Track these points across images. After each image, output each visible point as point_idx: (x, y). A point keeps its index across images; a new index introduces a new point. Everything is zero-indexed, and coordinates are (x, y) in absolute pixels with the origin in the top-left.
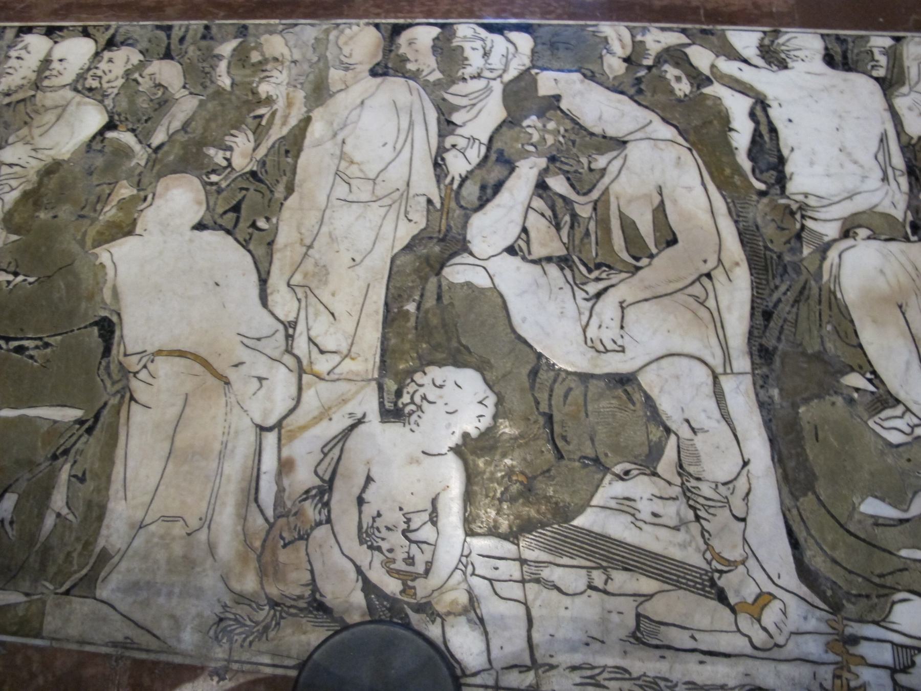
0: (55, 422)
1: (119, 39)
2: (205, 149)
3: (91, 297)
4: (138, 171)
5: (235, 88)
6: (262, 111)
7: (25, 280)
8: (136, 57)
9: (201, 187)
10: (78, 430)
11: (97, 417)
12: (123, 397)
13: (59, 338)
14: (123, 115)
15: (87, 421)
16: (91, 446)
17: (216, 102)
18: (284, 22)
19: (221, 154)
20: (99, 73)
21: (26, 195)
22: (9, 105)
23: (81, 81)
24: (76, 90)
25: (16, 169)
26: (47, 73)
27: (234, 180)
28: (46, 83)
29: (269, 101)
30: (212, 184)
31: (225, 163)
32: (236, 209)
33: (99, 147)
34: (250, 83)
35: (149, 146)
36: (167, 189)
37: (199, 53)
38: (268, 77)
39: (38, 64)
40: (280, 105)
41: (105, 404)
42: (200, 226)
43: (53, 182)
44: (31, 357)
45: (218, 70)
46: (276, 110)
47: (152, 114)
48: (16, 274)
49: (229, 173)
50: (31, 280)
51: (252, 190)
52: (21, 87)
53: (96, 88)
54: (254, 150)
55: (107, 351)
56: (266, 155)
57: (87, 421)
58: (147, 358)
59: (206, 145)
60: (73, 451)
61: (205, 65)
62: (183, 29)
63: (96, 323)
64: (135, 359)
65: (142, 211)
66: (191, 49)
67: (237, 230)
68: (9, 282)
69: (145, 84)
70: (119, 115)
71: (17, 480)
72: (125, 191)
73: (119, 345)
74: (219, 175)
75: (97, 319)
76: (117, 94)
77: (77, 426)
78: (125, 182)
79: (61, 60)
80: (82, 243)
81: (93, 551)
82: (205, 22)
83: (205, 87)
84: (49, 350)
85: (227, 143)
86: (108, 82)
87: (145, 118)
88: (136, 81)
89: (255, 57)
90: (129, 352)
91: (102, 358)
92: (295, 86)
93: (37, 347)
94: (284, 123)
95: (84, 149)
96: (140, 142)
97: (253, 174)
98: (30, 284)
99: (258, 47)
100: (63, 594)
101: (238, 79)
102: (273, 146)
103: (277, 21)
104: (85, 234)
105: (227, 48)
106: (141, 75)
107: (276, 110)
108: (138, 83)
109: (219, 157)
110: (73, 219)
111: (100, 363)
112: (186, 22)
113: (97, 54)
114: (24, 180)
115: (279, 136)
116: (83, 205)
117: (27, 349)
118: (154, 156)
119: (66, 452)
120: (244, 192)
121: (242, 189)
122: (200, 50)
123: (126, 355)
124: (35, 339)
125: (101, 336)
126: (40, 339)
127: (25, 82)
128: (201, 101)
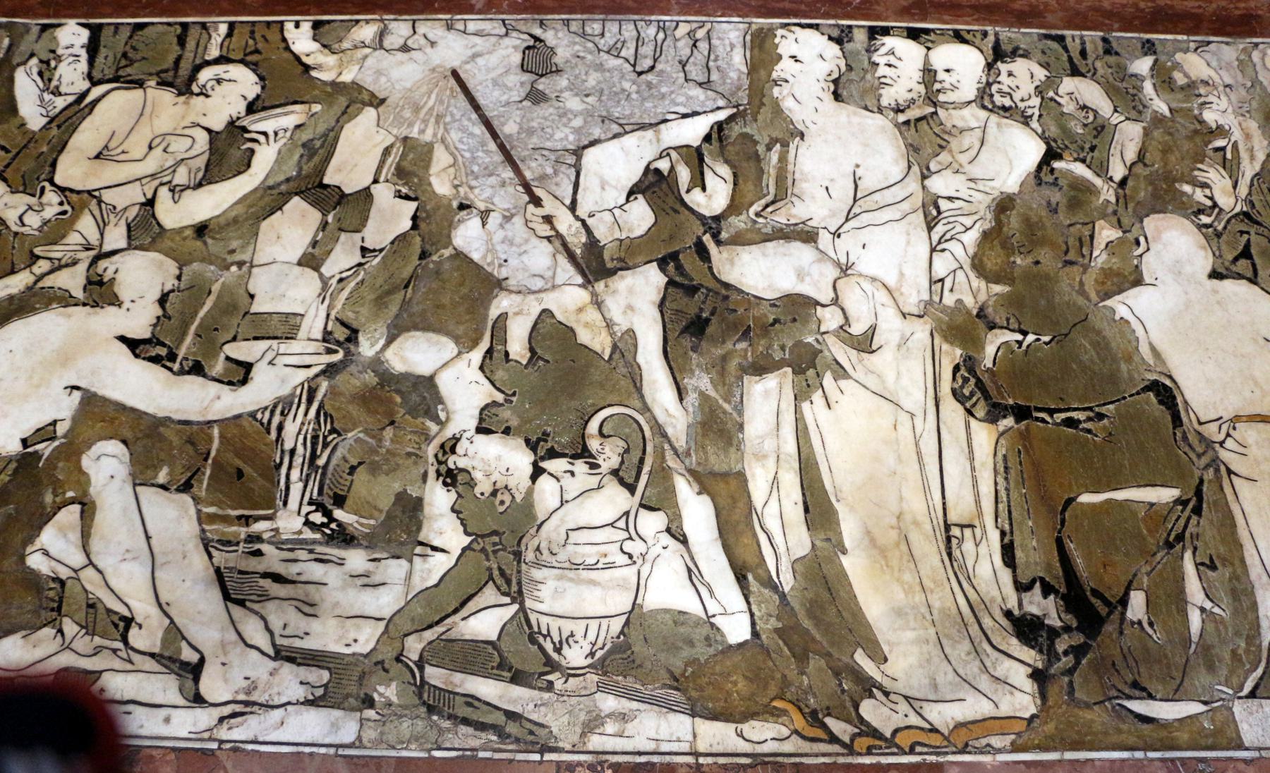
0: (1152, 505)
1: (1007, 48)
2: (1177, 185)
3: (1129, 359)
4: (1110, 210)
5: (1176, 114)
6: (1220, 143)
7: (1038, 340)
8: (1041, 74)
9: (1196, 230)
10: (1182, 512)
11: (1199, 493)
12: (1217, 470)
13: (1111, 407)
14: (1059, 142)
15: (1188, 501)
16: (1205, 526)
17: (1161, 130)
18: (1192, 38)
19: (1198, 190)
20: (1006, 89)
21: (986, 235)
22: (907, 123)
23: (986, 98)
24: (984, 107)
25: (958, 204)
26: (937, 86)
27: (1229, 221)
28: (942, 98)
29: (1220, 131)
30: (1207, 226)
31: (1209, 203)
32: (1246, 254)
33: (1050, 179)
34: (1190, 110)
35: (1111, 179)
36: (1159, 232)
37: (1110, 70)
38: (1206, 103)
39: (921, 73)
40: (1237, 135)
41: (1201, 481)
42: (1215, 275)
43: (1014, 222)
44: (1089, 431)
45: (1145, 91)
46: (1236, 142)
47: (1095, 142)
48: (1025, 333)
49: (1218, 214)
50: (1047, 339)
51: (1252, 232)
52: (913, 101)
53: (1010, 108)
54: (1235, 187)
55: (1177, 420)
56: (1250, 194)
57: (1188, 501)
58: (1227, 424)
59: (1175, 180)
60: (1187, 535)
61: (1125, 85)
62: (1078, 41)
63: (1147, 389)
64: (1213, 427)
65: (1141, 256)
66: (1098, 64)
67: (1259, 279)
68: (1020, 343)
69: (1069, 107)
70: (1055, 141)
71: (1135, 575)
72: (1107, 233)
73: (1187, 411)
74: (1209, 216)
75: (1147, 383)
76: (1040, 116)
77: (1180, 508)
78: (1102, 222)
79: (948, 71)
80: (1082, 292)
81: (1260, 645)
82: (1102, 34)
83: (1140, 112)
84: (1106, 421)
85: (1200, 179)
86: (1022, 100)
87: (1087, 146)
88: (1052, 99)
89: (1180, 79)
90: (1203, 420)
91: (1174, 428)
92: (1243, 115)
93: (1089, 419)
94: (1252, 158)
95: (1032, 181)
96: (1098, 175)
97: (1246, 215)
98: (1046, 343)
99: (1177, 66)
100: (1247, 697)
101: (1174, 105)
102: (1252, 185)
103: (1185, 37)
104: (1081, 283)
105: (1143, 66)
106: (1057, 94)
107: (1236, 142)
108: (1059, 104)
109: (1199, 195)
110: (1060, 265)
111: (1175, 434)
112: (1078, 33)
113: (990, 66)
114: (976, 217)
115: (1254, 173)
116: (1064, 248)
117: (1079, 421)
118: (1120, 191)
119: (1180, 538)
120: (1246, 237)
121: (1242, 232)
122: (1110, 67)
123: (1200, 423)
124: (1084, 409)
125: (1161, 402)
126: (1090, 409)
127: (914, 95)
128: (1144, 128)
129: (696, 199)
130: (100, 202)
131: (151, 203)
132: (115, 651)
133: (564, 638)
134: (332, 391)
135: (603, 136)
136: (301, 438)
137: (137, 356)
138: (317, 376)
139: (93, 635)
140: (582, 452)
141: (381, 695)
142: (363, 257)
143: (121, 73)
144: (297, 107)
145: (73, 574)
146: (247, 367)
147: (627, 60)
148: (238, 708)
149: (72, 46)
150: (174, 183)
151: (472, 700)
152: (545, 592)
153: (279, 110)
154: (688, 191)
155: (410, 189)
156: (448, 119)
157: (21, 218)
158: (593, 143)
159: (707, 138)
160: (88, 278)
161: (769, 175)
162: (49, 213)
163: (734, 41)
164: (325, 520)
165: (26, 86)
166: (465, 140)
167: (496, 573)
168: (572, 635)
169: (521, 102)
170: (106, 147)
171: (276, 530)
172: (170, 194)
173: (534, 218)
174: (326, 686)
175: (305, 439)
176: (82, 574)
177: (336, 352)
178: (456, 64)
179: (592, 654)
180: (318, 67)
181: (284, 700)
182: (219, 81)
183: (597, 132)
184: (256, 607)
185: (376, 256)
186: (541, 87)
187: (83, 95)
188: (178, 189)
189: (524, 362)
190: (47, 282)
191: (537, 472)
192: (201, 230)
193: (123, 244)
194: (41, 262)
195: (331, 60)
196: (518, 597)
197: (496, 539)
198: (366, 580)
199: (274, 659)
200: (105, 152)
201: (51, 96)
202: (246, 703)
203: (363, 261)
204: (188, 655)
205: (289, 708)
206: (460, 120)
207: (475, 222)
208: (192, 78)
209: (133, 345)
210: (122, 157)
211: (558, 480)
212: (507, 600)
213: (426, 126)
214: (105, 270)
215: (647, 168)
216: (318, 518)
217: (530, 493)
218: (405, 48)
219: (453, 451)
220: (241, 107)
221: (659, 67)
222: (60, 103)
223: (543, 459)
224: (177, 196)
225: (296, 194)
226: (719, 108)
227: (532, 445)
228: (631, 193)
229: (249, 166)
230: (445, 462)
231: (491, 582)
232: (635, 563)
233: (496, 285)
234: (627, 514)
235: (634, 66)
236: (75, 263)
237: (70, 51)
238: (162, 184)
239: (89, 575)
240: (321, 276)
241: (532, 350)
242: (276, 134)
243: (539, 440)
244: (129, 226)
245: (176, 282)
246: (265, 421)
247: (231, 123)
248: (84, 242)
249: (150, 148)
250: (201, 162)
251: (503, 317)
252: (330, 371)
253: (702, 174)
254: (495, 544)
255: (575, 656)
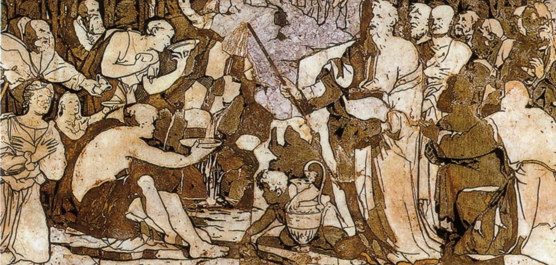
129: (340, 81)
130: (122, 83)
131: (141, 84)
132: (161, 244)
133: (300, 234)
134: (220, 156)
135: (307, 55)
136: (211, 174)
137: (149, 145)
138: (214, 151)
139: (153, 239)
140: (304, 177)
141: (246, 254)
142: (224, 106)
143: (116, 23)
144: (191, 41)
145: (142, 220)
146: (189, 148)
147: (315, 19)
148: (202, 259)
149: (93, 10)
150: (149, 75)
151: (273, 255)
152: (293, 221)
153: (183, 43)
154: (337, 78)
155: (238, 77)
156: (249, 47)
157: (93, 89)
158: (303, 58)
159: (344, 55)
160: (124, 114)
161: (367, 70)
162: (104, 87)
163: (356, 8)
164: (223, 200)
165: (80, 31)
166: (256, 57)
167: (278, 216)
168: (302, 234)
169: (275, 39)
170: (118, 58)
171: (208, 204)
172: (148, 80)
173: (283, 90)
174: (228, 252)
175: (213, 174)
176: (146, 220)
177: (219, 142)
178: (249, 21)
179: (308, 240)
180: (196, 22)
181: (216, 256)
182: (157, 28)
183: (304, 53)
184: (204, 229)
185: (228, 106)
186: (282, 32)
187: (104, 35)
188: (151, 78)
189: (283, 145)
190: (110, 116)
191: (289, 183)
192: (163, 95)
193: (134, 101)
194: (105, 108)
195: (200, 19)
196: (285, 224)
197: (277, 205)
198: (237, 219)
199: (212, 244)
200: (119, 61)
201: (91, 35)
202: (205, 258)
203: (224, 107)
204: (184, 244)
205: (218, 259)
206: (253, 47)
207: (263, 92)
208: (146, 27)
209: (147, 140)
210: (125, 64)
211: (296, 186)
212: (282, 224)
213: (241, 51)
214: (130, 111)
215: (323, 68)
216: (220, 200)
217: (287, 189)
218: (228, 13)
219: (262, 177)
220: (167, 41)
221: (327, 22)
222: (96, 39)
223: (291, 179)
224: (151, 81)
225: (196, 80)
226: (349, 41)
227: (287, 174)
228: (317, 79)
229: (176, 68)
230: (259, 181)
231: (276, 220)
232: (320, 212)
233: (273, 117)
234: (317, 196)
235: (317, 21)
236: (118, 109)
237: (93, 13)
238: (144, 75)
239: (147, 220)
240: (210, 113)
241: (285, 141)
242: (184, 53)
243: (289, 172)
244: (135, 93)
245: (158, 116)
246: (198, 167)
247: (165, 49)
248: (119, 100)
249: (136, 59)
250: (157, 66)
251: (275, 128)
252: (218, 149)
253: (342, 70)
254: (277, 207)
255: (303, 240)
